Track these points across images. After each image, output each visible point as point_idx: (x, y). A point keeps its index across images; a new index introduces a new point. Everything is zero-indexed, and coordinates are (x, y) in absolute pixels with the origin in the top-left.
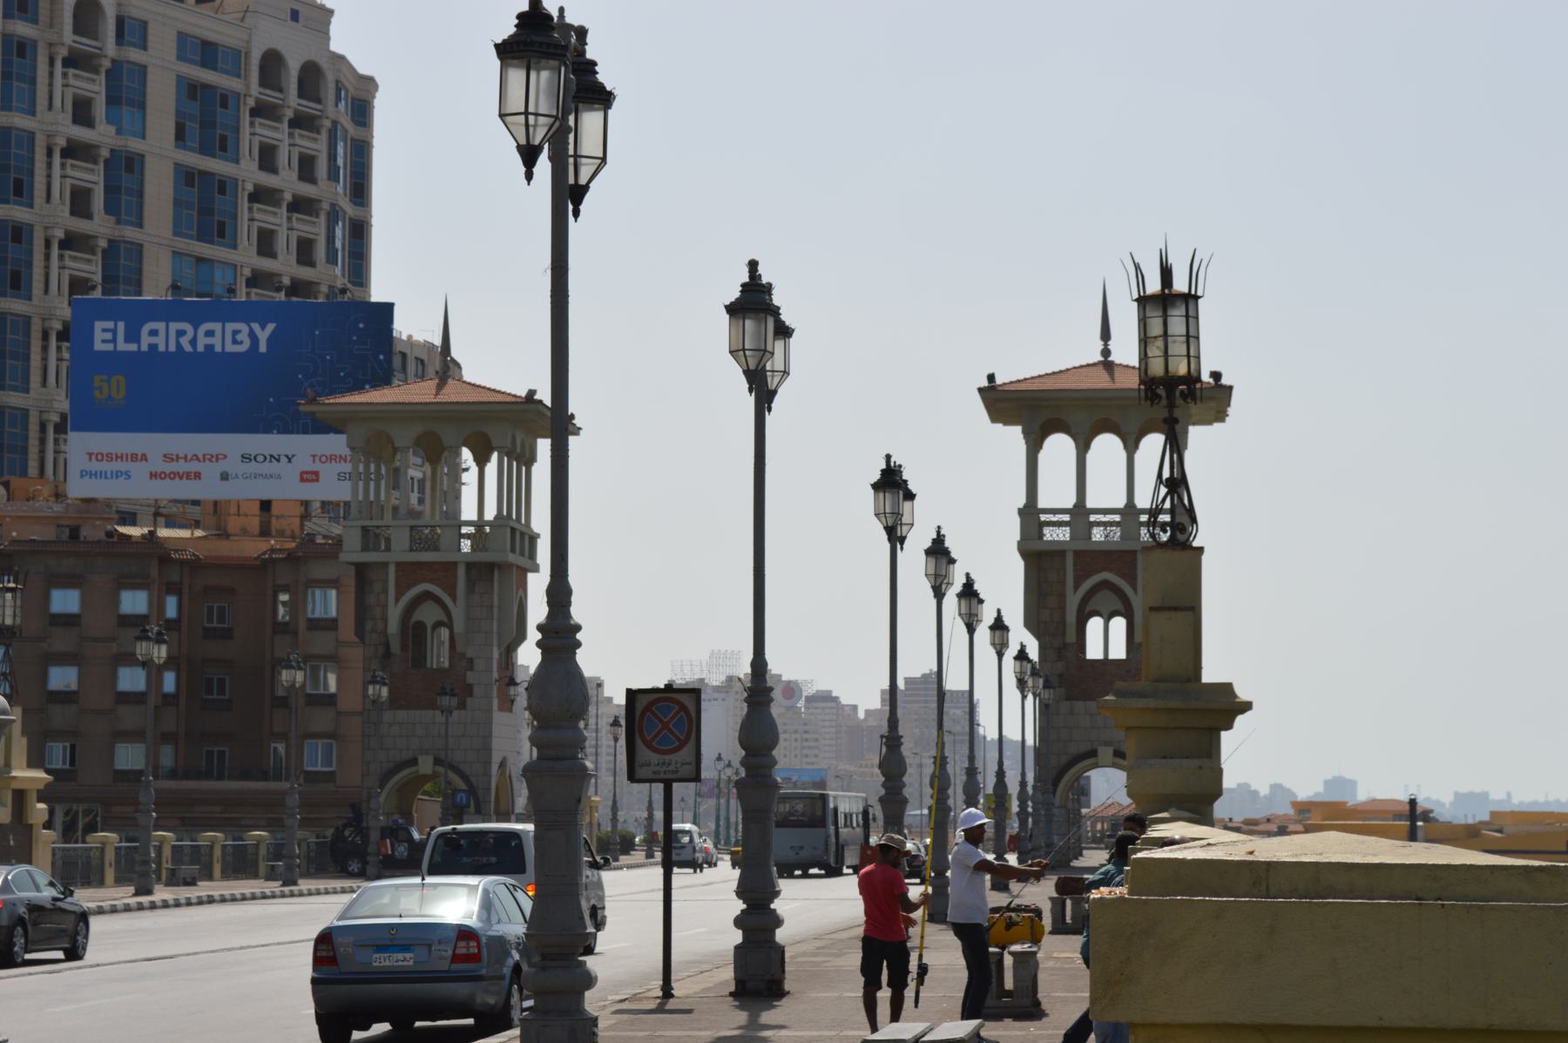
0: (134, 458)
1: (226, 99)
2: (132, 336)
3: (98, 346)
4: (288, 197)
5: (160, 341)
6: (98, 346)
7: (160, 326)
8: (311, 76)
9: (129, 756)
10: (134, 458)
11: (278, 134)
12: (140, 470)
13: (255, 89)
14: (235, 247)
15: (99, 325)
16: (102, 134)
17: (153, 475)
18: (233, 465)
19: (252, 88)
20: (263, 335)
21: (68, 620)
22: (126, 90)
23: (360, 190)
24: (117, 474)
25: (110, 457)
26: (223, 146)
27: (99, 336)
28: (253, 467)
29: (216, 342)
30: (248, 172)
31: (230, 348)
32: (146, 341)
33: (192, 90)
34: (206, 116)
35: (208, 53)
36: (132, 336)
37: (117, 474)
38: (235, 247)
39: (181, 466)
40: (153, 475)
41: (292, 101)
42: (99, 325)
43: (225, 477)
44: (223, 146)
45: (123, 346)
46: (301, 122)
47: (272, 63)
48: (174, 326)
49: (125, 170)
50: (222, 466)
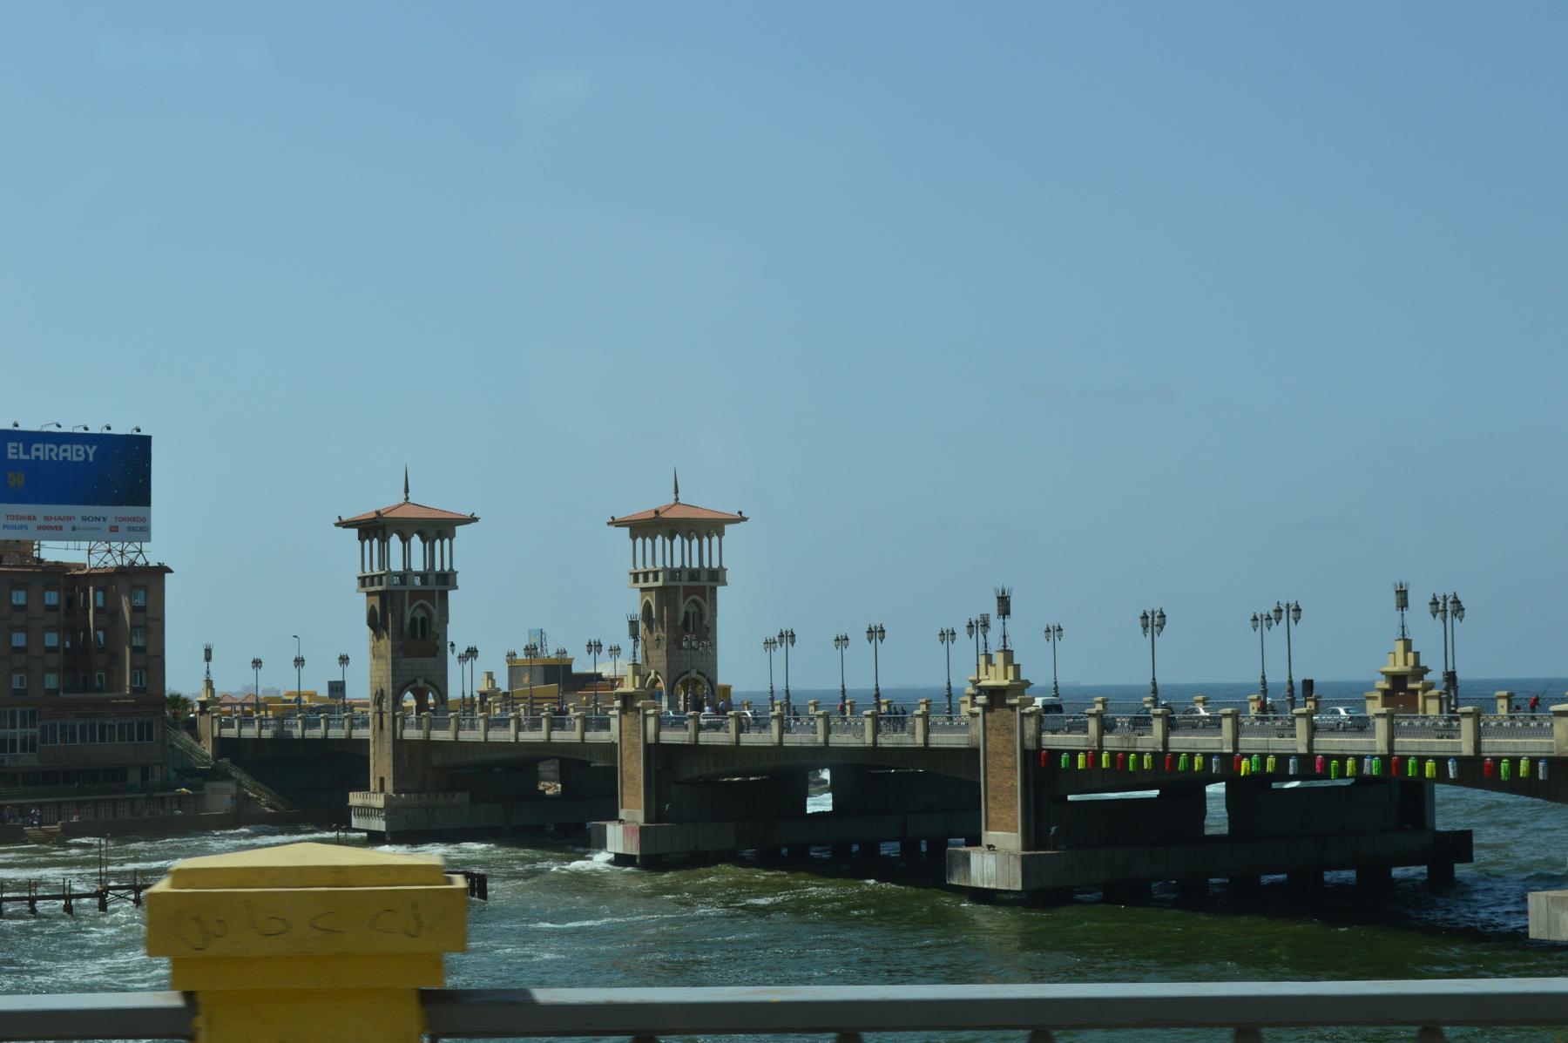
0: (29, 518)
2: (27, 451)
3: (10, 456)
5: (40, 454)
6: (10, 456)
7: (40, 446)
9: (51, 681)
10: (29, 518)
12: (32, 525)
15: (10, 445)
17: (39, 528)
18: (78, 522)
20: (91, 452)
21: (22, 608)
24: (21, 527)
25: (17, 518)
27: (10, 451)
28: (88, 524)
29: (68, 455)
31: (75, 459)
32: (34, 454)
36: (27, 451)
37: (21, 527)
39: (53, 523)
40: (39, 528)
42: (10, 445)
43: (74, 529)
45: (23, 457)
48: (48, 446)
50: (74, 523)
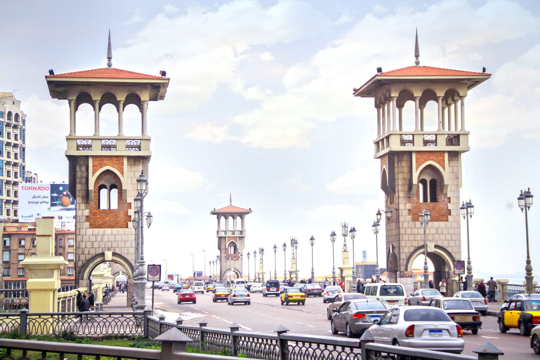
4: (13, 144)
8: (17, 115)
11: (10, 130)
13: (7, 121)
14: (3, 156)
19: (5, 120)
38: (3, 156)
41: (13, 122)
46: (15, 127)
47: (10, 113)
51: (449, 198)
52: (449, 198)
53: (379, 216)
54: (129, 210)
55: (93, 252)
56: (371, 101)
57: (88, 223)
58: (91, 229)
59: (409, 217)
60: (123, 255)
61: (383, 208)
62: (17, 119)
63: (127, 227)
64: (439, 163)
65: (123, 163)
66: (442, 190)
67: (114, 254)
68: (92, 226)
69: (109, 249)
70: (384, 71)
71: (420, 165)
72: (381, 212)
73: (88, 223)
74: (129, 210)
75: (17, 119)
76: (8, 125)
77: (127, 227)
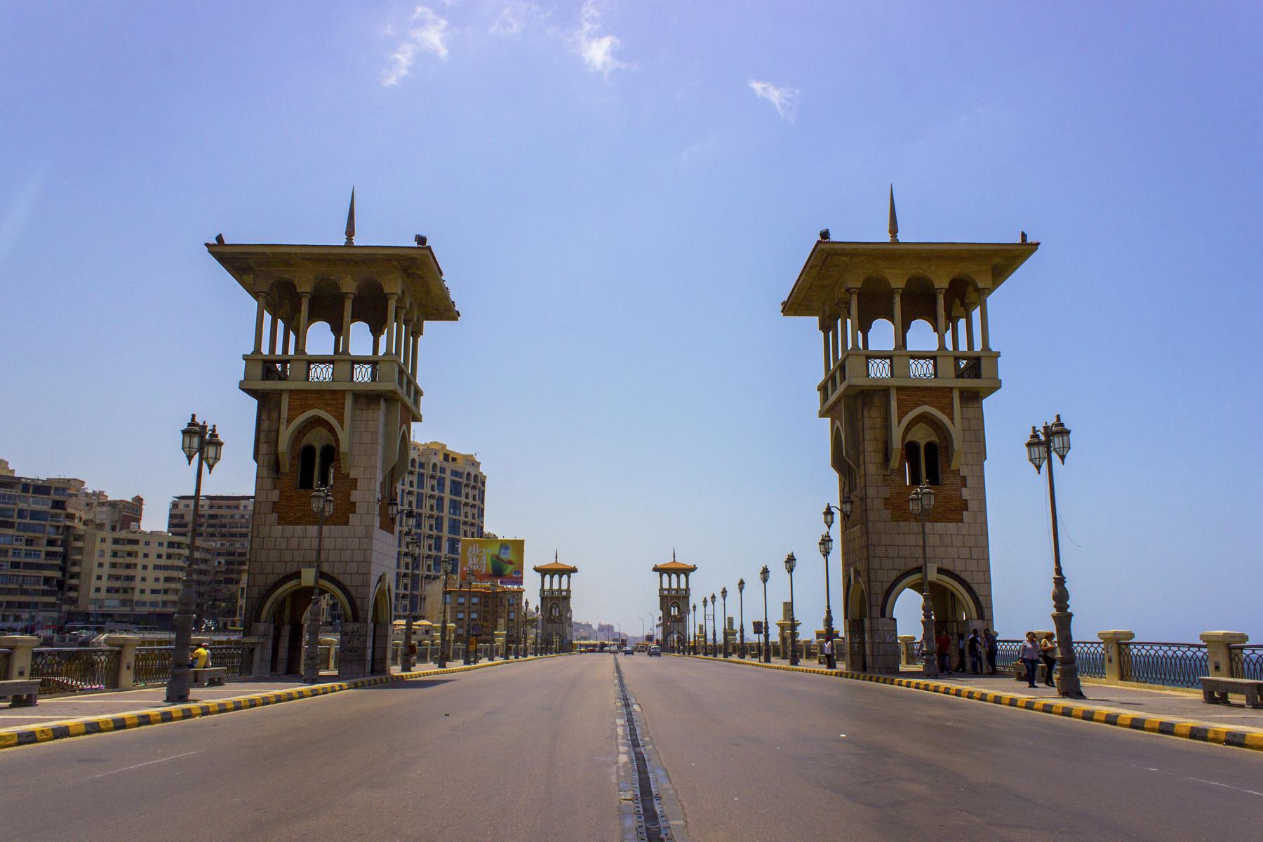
1: (460, 483)
8: (476, 476)
11: (469, 490)
16: (436, 493)
19: (464, 481)
22: (441, 482)
23: (483, 502)
26: (459, 494)
30: (463, 499)
33: (453, 482)
34: (456, 488)
35: (455, 473)
44: (459, 494)
46: (474, 488)
47: (469, 474)
49: (441, 500)
51: (964, 477)
52: (964, 477)
53: (829, 517)
54: (353, 492)
55: (281, 570)
56: (811, 323)
57: (275, 516)
58: (280, 527)
59: (887, 514)
60: (336, 576)
61: (836, 502)
62: (475, 481)
63: (347, 523)
64: (941, 409)
65: (343, 404)
66: (949, 461)
67: (322, 575)
68: (283, 520)
69: (310, 565)
70: (833, 238)
71: (906, 414)
72: (833, 510)
73: (275, 516)
74: (353, 492)
75: (475, 481)
76: (466, 486)
77: (347, 523)
